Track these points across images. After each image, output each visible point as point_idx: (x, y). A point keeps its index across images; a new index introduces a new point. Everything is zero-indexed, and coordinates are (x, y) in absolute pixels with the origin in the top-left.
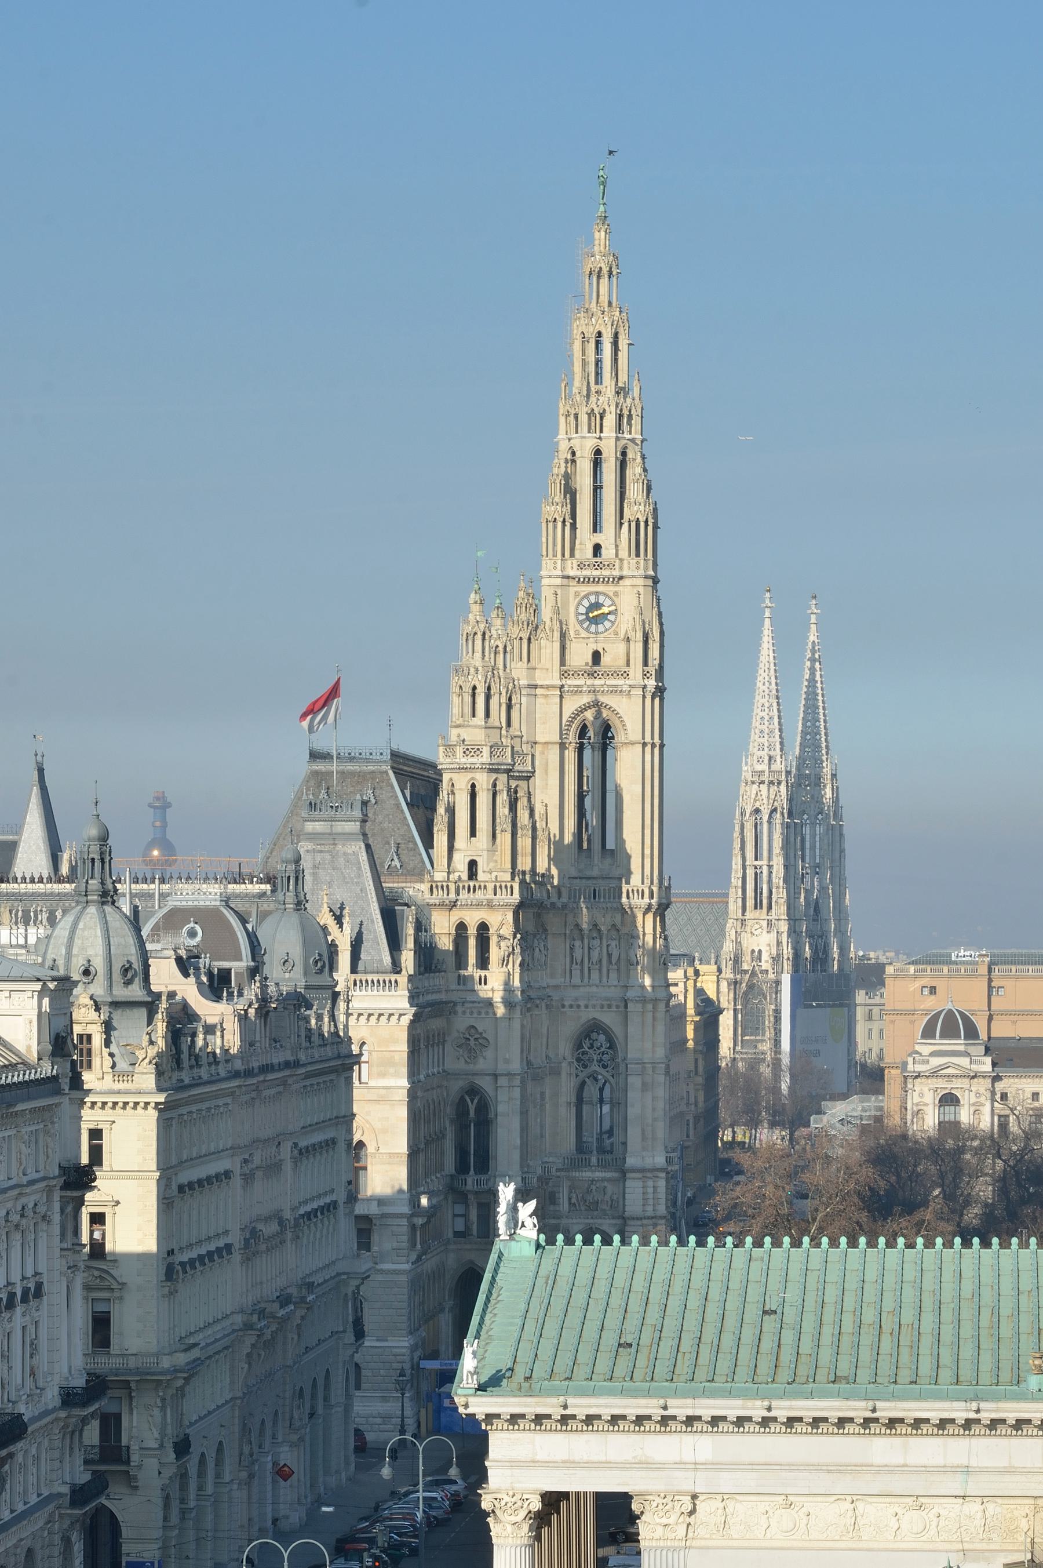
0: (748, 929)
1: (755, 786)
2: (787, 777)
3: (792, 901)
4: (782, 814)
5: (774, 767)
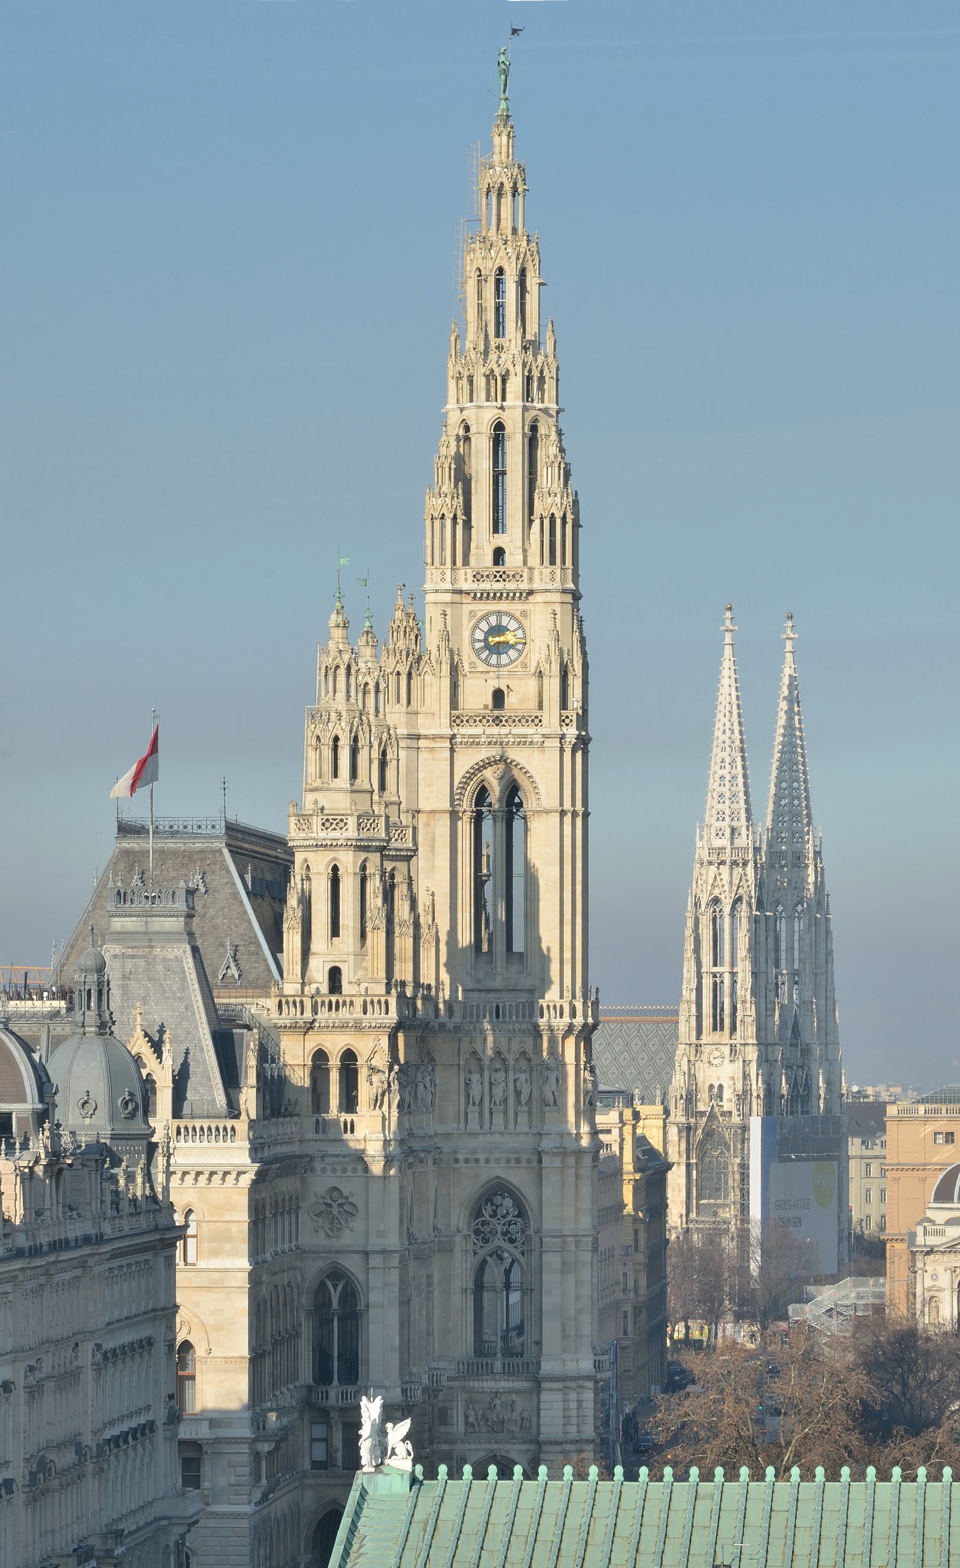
0: (705, 1057)
1: (713, 868)
2: (755, 855)
3: (763, 1020)
4: (750, 904)
5: (738, 843)
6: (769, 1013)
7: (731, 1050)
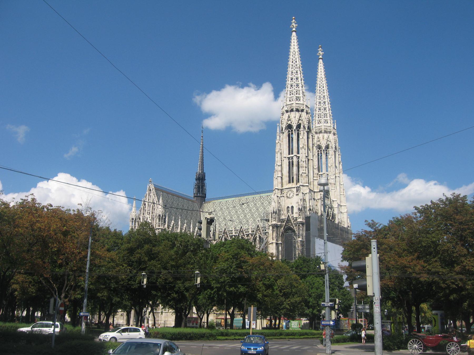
0: (285, 195)
6: (315, 178)
7: (297, 190)
